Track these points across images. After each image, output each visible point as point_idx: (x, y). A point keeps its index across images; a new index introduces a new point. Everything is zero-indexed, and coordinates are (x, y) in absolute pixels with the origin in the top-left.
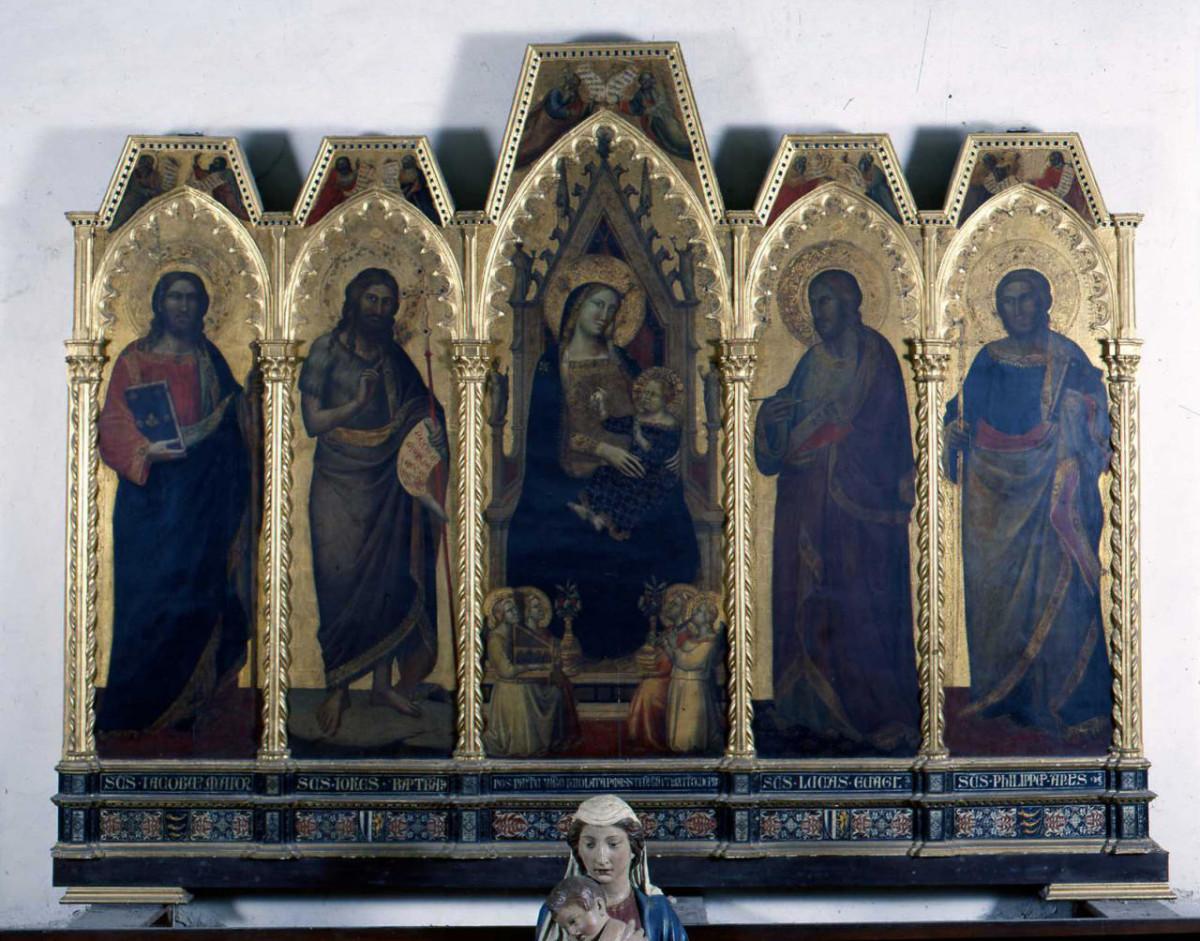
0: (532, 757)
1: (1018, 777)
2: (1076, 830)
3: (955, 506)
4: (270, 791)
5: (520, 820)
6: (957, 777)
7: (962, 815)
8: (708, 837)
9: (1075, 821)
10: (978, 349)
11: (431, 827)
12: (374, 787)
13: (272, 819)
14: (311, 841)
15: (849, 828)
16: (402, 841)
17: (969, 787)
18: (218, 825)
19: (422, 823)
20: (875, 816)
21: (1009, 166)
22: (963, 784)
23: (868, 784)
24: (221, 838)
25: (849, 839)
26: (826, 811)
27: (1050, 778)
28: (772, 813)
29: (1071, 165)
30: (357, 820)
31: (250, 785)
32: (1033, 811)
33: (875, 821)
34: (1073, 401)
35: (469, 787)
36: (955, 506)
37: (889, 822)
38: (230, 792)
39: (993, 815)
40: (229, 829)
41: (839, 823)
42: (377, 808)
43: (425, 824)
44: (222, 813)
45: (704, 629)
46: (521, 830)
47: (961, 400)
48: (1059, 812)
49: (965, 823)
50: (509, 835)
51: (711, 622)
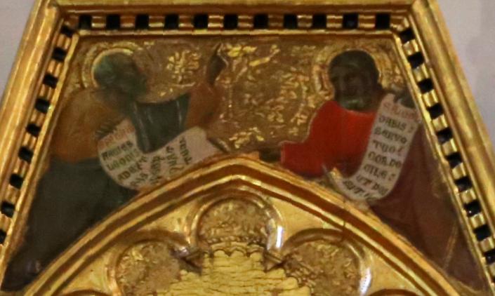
21: (185, 98)
29: (406, 98)
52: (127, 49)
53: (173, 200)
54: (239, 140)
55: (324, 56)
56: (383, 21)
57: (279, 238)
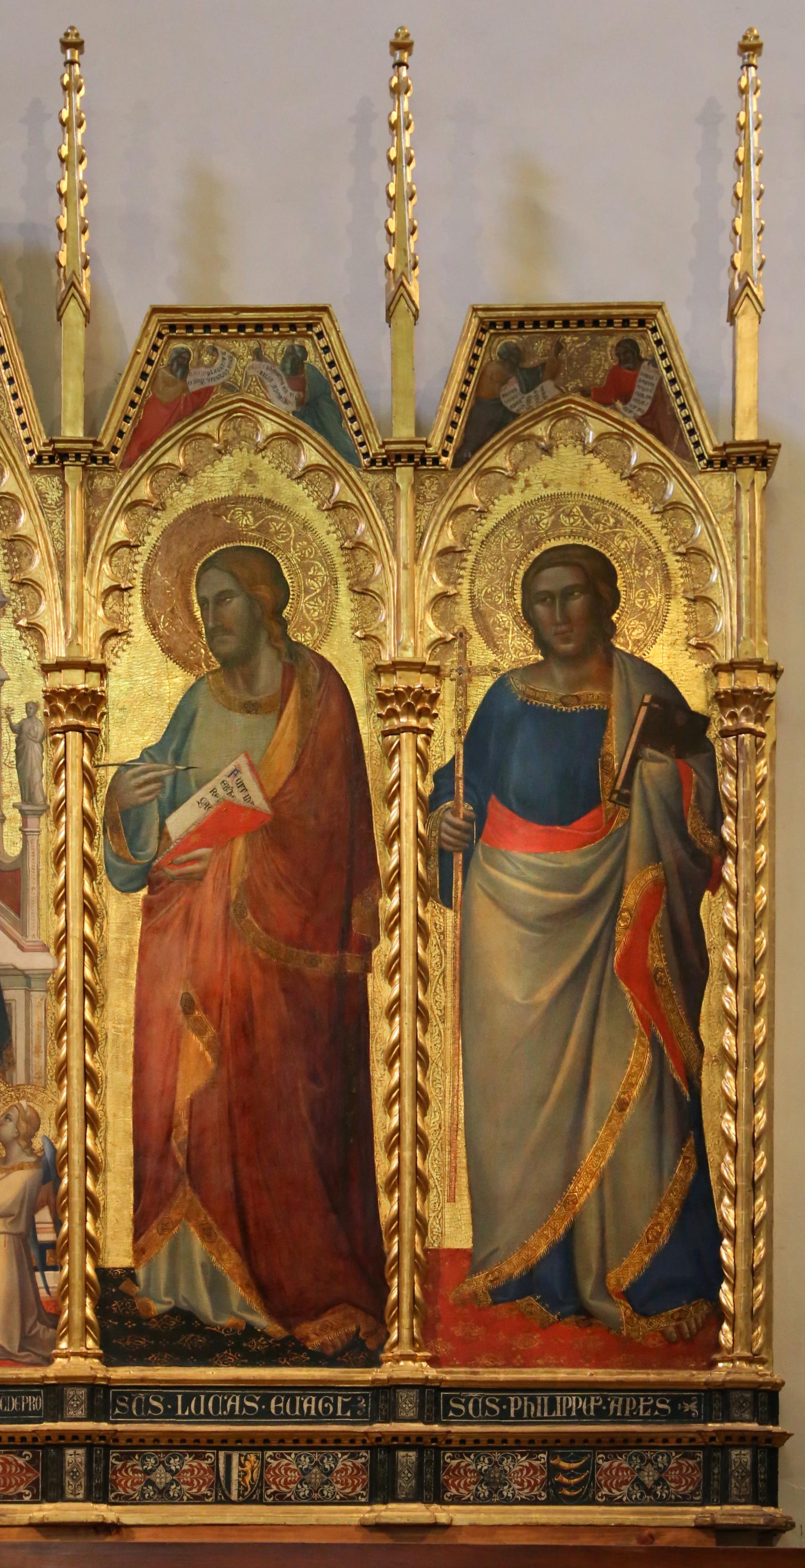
1: (552, 1401)
2: (649, 1491)
3: (449, 945)
6: (447, 1399)
7: (454, 1463)
8: (20, 1495)
9: (649, 1477)
10: (488, 682)
15: (262, 1483)
17: (467, 1416)
20: (305, 1463)
21: (543, 365)
22: (457, 1411)
23: (293, 1409)
25: (260, 1501)
26: (222, 1455)
27: (606, 1403)
28: (129, 1457)
32: (576, 1458)
33: (305, 1472)
34: (655, 768)
36: (449, 945)
37: (329, 1473)
39: (507, 1464)
41: (243, 1475)
45: (16, 1149)
47: (460, 773)
48: (621, 1461)
49: (459, 1477)
51: (29, 1137)
52: (513, 340)
53: (537, 418)
54: (571, 386)
55: (612, 342)
56: (642, 323)
57: (591, 438)
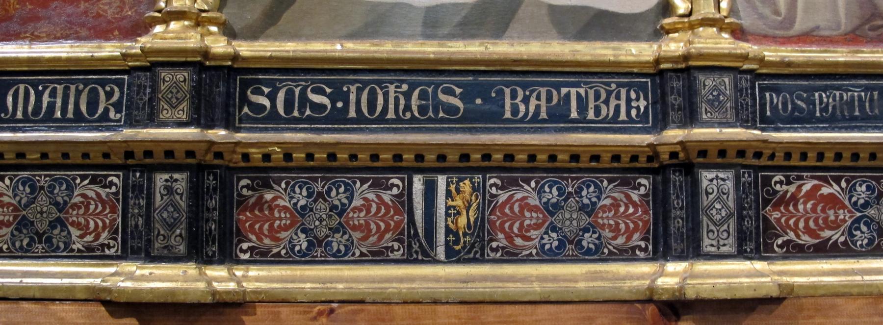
0: (853, 38)
4: (166, 115)
5: (832, 201)
11: (606, 218)
12: (451, 110)
13: (170, 190)
14: (278, 260)
16: (528, 260)
18: (29, 213)
19: (582, 208)
24: (39, 247)
30: (405, 199)
31: (118, 106)
35: (715, 103)
38: (64, 124)
40: (60, 223)
42: (463, 164)
43: (589, 210)
44: (43, 179)
46: (835, 226)
50: (806, 239)
